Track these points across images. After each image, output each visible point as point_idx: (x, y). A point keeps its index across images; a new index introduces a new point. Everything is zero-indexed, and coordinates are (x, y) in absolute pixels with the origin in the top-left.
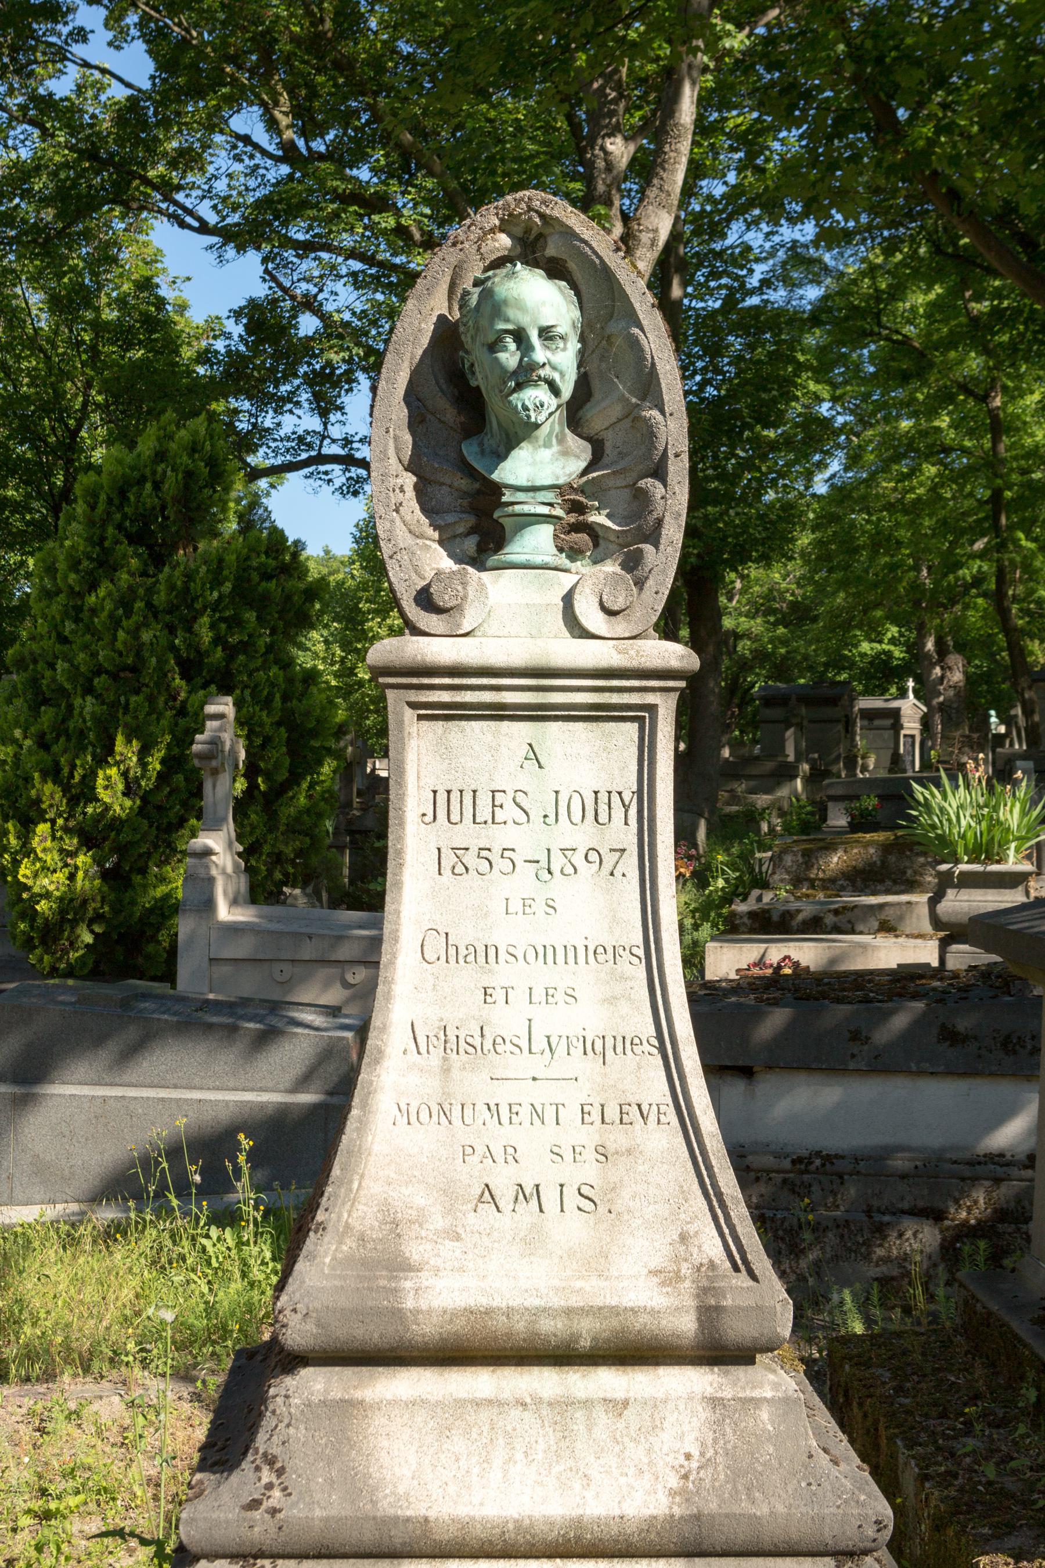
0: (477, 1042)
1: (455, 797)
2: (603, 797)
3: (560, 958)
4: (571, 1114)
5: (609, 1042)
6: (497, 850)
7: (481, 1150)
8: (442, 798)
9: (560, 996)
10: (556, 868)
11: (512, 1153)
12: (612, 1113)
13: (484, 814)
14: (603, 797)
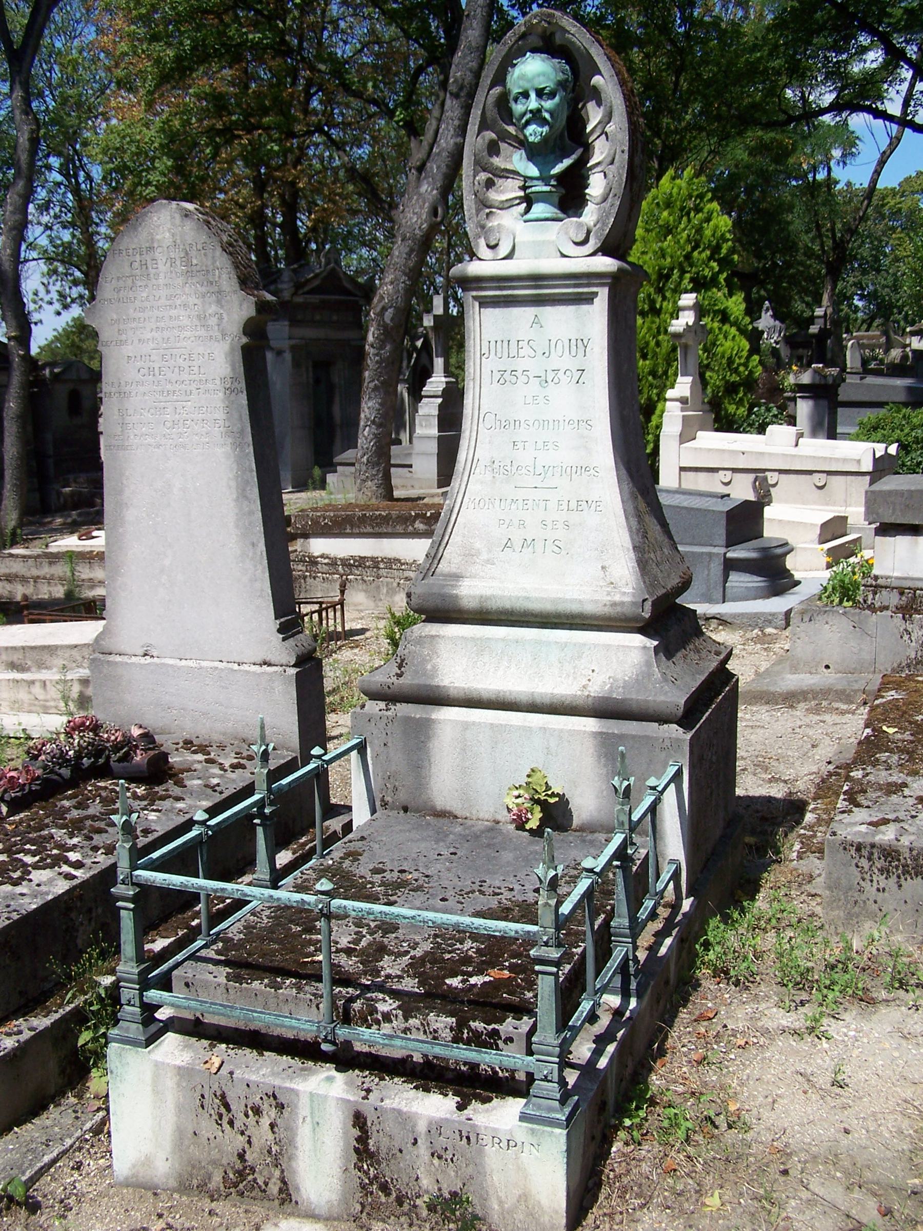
0: (508, 468)
1: (499, 343)
2: (573, 342)
3: (551, 426)
4: (552, 505)
5: (574, 469)
6: (520, 371)
7: (507, 522)
8: (493, 343)
9: (550, 445)
10: (549, 380)
11: (522, 524)
12: (573, 505)
13: (513, 352)
14: (573, 342)
